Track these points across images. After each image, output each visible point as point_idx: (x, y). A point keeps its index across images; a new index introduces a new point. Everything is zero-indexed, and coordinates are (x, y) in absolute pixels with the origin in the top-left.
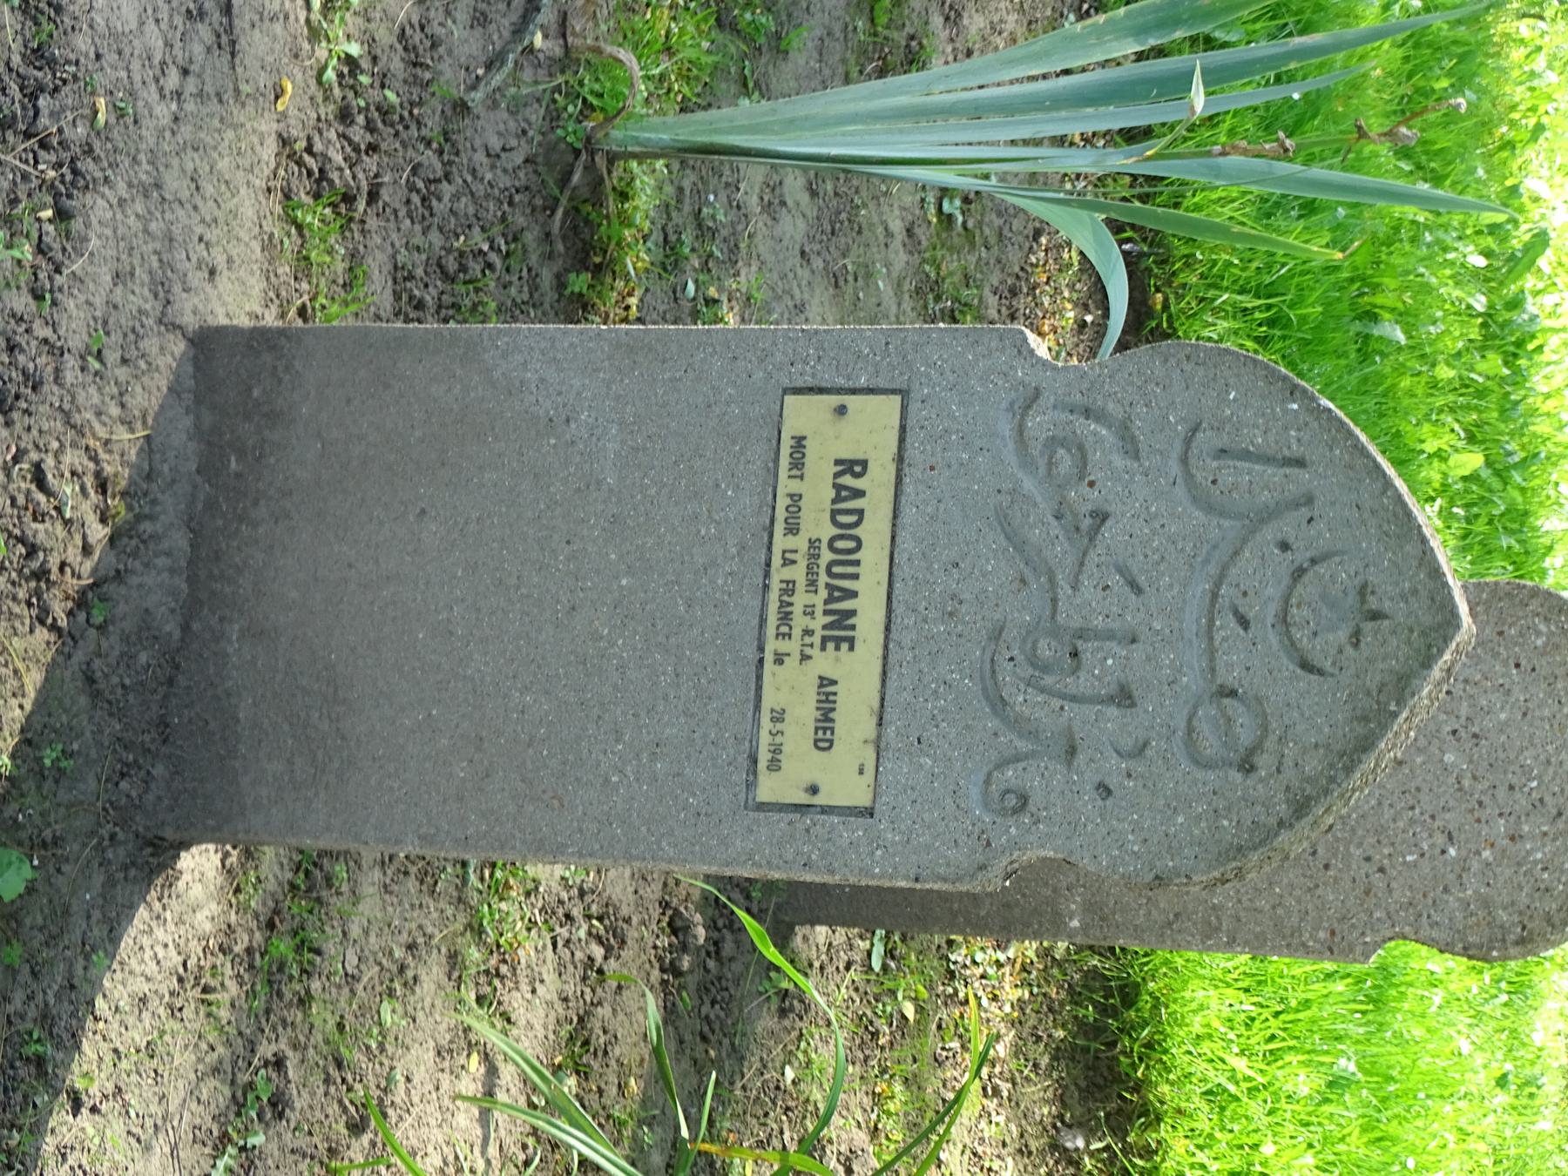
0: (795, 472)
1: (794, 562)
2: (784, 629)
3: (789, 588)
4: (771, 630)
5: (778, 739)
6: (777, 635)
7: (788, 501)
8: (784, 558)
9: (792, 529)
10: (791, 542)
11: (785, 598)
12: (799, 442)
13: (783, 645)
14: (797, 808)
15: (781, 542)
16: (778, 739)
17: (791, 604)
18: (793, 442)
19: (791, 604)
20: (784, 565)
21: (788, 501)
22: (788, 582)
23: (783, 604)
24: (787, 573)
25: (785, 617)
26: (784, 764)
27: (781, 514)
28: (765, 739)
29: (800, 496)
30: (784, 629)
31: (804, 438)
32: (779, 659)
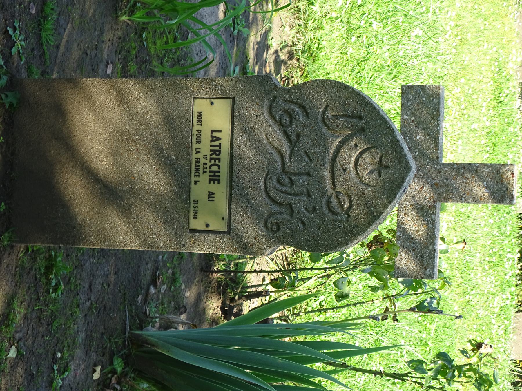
0: (199, 123)
1: (199, 152)
2: (197, 174)
3: (198, 161)
4: (193, 174)
5: (196, 209)
6: (195, 176)
7: (197, 133)
8: (196, 151)
9: (199, 142)
10: (198, 146)
11: (197, 164)
12: (200, 113)
13: (197, 179)
15: (195, 146)
17: (199, 166)
19: (199, 166)
20: (196, 153)
21: (197, 133)
22: (198, 159)
23: (196, 166)
25: (197, 170)
26: (197, 217)
27: (195, 137)
28: (192, 209)
30: (197, 174)
31: (202, 112)
32: (196, 183)
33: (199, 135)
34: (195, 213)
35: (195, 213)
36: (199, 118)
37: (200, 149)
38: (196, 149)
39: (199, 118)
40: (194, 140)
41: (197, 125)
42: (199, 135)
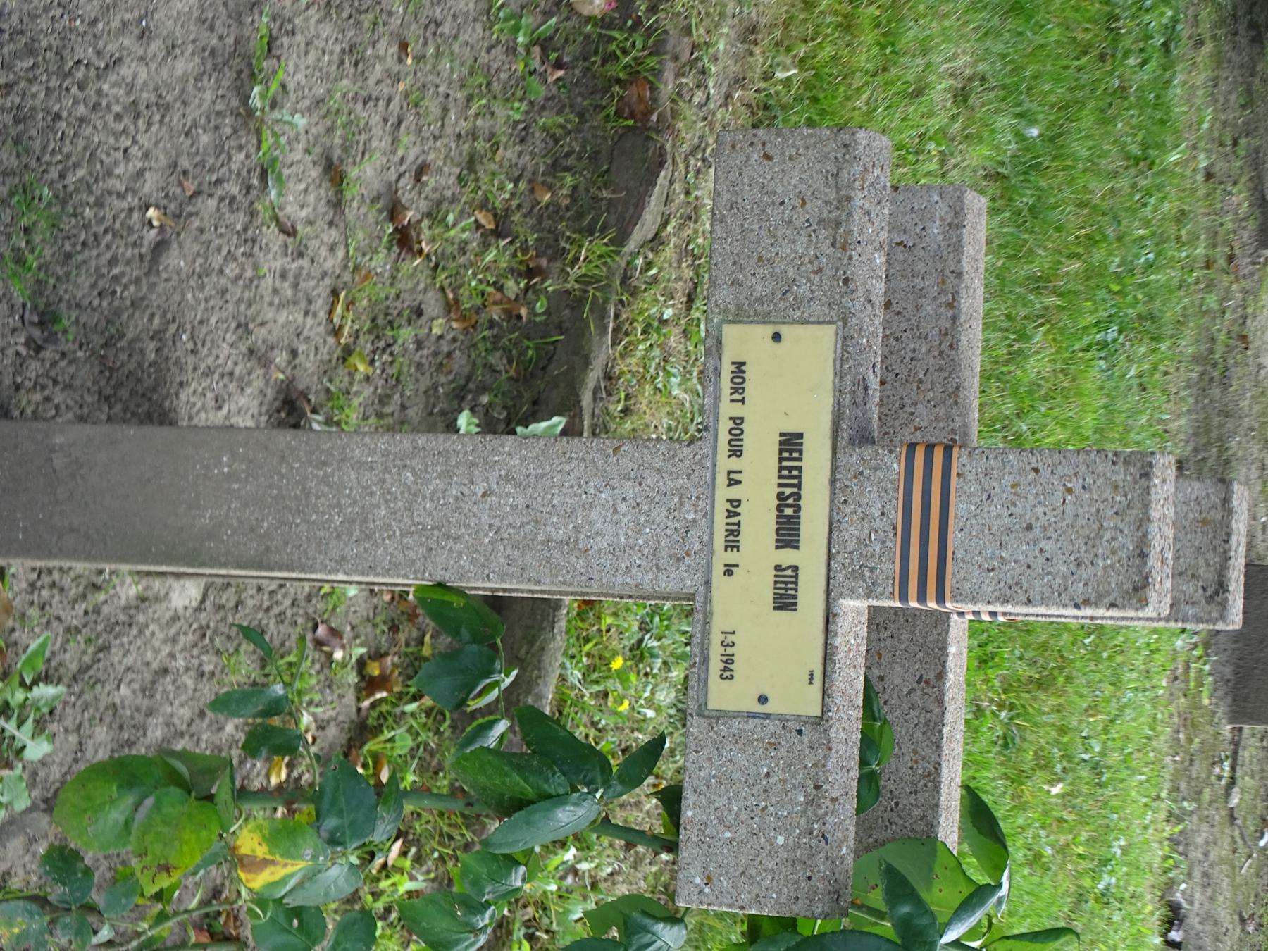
0: (736, 396)
1: (740, 482)
7: (731, 425)
8: (730, 479)
9: (736, 452)
10: (734, 463)
12: (739, 367)
14: (752, 715)
15: (725, 463)
16: (730, 650)
18: (733, 368)
21: (731, 425)
24: (734, 493)
27: (724, 437)
29: (742, 419)
31: (744, 364)
33: (738, 432)
34: (726, 662)
35: (726, 662)
36: (737, 380)
37: (740, 472)
38: (730, 472)
39: (737, 380)
40: (723, 447)
41: (732, 401)
42: (738, 432)
